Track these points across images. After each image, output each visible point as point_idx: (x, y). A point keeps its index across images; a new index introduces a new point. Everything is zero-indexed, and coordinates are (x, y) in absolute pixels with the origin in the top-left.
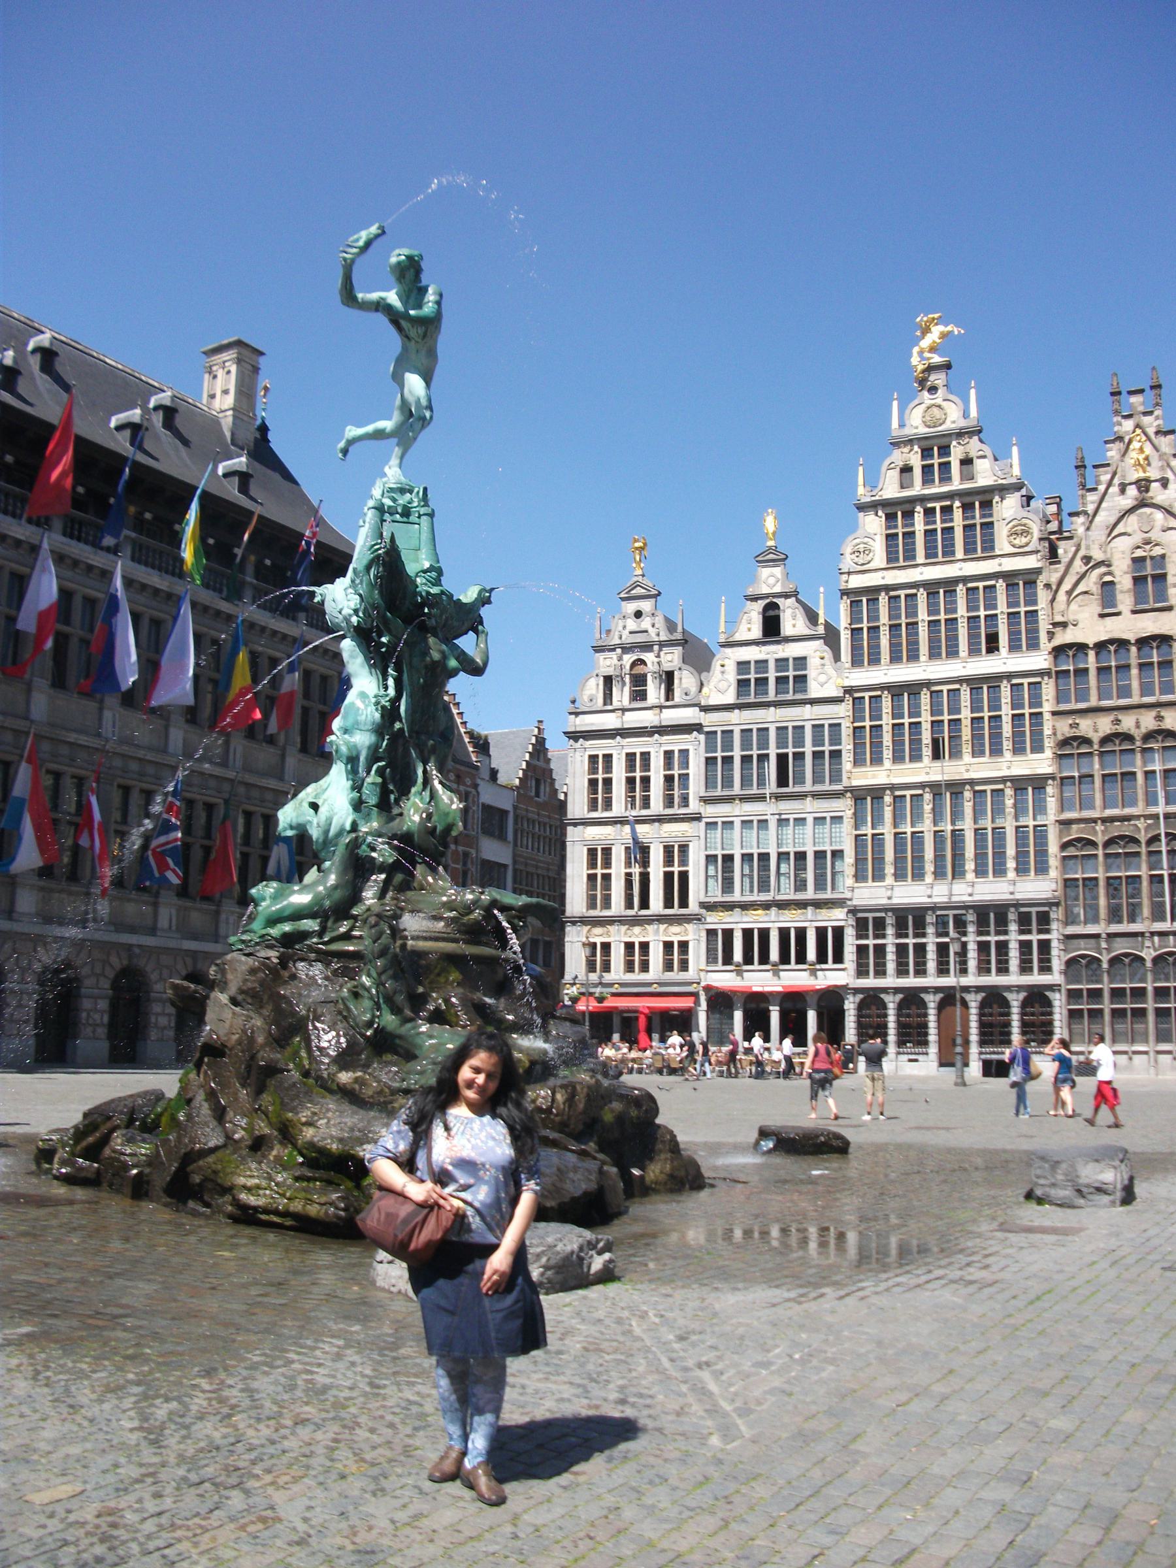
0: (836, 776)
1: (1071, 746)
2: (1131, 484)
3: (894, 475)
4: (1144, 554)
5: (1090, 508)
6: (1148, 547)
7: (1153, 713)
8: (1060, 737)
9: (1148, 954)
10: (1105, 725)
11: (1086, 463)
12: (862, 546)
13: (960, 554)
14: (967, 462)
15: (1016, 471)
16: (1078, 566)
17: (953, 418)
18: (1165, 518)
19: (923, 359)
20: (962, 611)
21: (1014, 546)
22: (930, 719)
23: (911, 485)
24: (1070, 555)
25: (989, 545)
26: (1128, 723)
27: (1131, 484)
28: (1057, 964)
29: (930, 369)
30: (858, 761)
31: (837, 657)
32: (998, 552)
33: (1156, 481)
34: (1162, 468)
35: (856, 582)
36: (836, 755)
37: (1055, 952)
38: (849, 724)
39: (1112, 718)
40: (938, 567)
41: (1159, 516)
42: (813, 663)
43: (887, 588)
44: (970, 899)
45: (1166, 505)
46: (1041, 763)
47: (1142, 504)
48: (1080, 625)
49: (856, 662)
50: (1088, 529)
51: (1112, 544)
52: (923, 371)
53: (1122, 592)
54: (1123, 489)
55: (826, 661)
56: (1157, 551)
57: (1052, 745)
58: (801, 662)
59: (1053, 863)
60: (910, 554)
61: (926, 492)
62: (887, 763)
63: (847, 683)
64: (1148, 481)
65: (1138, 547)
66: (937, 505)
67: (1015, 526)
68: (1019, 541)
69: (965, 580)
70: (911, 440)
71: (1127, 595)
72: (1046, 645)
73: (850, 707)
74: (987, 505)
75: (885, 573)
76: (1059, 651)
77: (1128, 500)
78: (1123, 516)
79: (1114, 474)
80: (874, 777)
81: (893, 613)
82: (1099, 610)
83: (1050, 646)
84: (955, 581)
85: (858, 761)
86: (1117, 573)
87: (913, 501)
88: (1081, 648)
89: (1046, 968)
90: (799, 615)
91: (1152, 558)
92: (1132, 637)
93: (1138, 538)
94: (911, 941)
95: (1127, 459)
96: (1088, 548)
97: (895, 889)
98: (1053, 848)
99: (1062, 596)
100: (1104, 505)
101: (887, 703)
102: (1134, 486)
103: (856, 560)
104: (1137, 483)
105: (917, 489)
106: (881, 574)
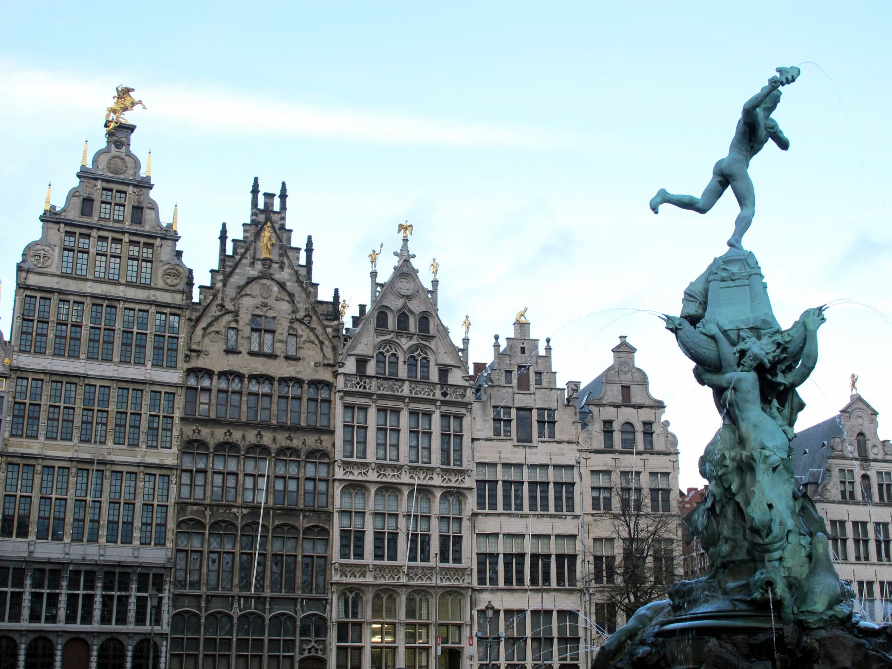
1: (192, 446)
2: (259, 260)
3: (78, 202)
4: (261, 313)
5: (228, 270)
6: (265, 309)
7: (256, 432)
8: (185, 438)
9: (236, 613)
10: (220, 434)
12: (42, 252)
14: (138, 210)
16: (214, 311)
18: (279, 292)
21: (167, 284)
22: (82, 406)
23: (90, 215)
24: (208, 301)
26: (237, 435)
27: (259, 260)
28: (166, 617)
33: (276, 263)
34: (281, 255)
35: (34, 280)
37: (165, 608)
38: (11, 399)
39: (225, 430)
40: (103, 285)
41: (275, 289)
43: (60, 292)
44: (101, 558)
45: (281, 281)
46: (169, 457)
47: (264, 275)
48: (210, 356)
50: (224, 285)
51: (240, 302)
52: (115, 128)
53: (243, 338)
54: (252, 264)
56: (271, 314)
57: (179, 443)
59: (170, 536)
62: (42, 438)
63: (15, 363)
64: (271, 260)
65: (258, 307)
66: (110, 235)
67: (168, 269)
68: (171, 281)
69: (126, 300)
71: (246, 340)
72: (183, 366)
73: (15, 384)
75: (59, 279)
76: (190, 372)
77: (253, 273)
78: (250, 282)
79: (247, 250)
80: (28, 447)
82: (225, 347)
83: (186, 366)
84: (117, 300)
86: (241, 323)
88: (209, 373)
89: (158, 621)
91: (266, 317)
92: (246, 372)
93: (259, 301)
94: (45, 591)
95: (258, 242)
96: (223, 299)
97: (38, 545)
98: (171, 525)
99: (199, 331)
100: (237, 270)
101: (114, 394)
102: (260, 262)
103: (35, 263)
104: (265, 259)
106: (56, 279)
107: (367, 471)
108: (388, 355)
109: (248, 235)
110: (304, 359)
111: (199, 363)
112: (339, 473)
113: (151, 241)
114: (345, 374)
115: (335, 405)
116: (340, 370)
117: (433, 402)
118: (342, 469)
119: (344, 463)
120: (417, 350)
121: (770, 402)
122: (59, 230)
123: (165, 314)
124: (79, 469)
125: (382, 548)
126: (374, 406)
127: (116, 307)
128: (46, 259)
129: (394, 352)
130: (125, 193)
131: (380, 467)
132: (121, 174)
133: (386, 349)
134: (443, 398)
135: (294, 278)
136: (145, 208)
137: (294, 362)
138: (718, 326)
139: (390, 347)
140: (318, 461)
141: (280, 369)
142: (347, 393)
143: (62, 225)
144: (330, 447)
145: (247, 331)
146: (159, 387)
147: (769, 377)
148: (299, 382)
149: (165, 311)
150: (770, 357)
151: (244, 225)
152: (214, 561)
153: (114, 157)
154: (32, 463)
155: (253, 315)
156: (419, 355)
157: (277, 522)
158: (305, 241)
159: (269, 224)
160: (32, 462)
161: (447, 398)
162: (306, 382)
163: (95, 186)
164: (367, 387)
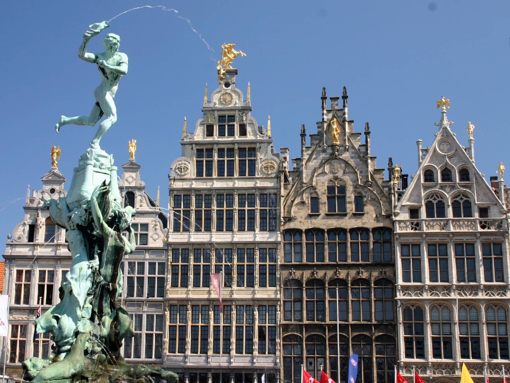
0: (162, 292)
11: (306, 133)
12: (183, 165)
13: (236, 175)
15: (269, 133)
17: (237, 102)
18: (346, 167)
19: (223, 67)
20: (236, 207)
25: (252, 172)
29: (229, 72)
30: (174, 285)
31: (165, 226)
32: (257, 176)
35: (178, 185)
36: (162, 281)
42: (151, 227)
47: (333, 157)
48: (299, 219)
49: (177, 229)
55: (158, 227)
58: (145, 226)
60: (209, 174)
61: (220, 139)
62: (190, 287)
63: (171, 240)
70: (214, 111)
74: (253, 151)
75: (194, 182)
81: (198, 205)
85: (174, 285)
87: (212, 143)
88: (298, 232)
90: (144, 201)
93: (331, 176)
102: (330, 148)
105: (216, 138)
107: (422, 292)
108: (435, 202)
109: (320, 130)
110: (368, 213)
111: (292, 225)
112: (400, 296)
113: (253, 146)
114: (400, 222)
115: (394, 244)
116: (397, 218)
117: (474, 234)
118: (401, 292)
119: (402, 287)
120: (459, 196)
121: (94, 247)
122: (192, 149)
123: (266, 194)
124: (215, 306)
125: (439, 349)
126: (424, 242)
127: (232, 195)
128: (186, 169)
129: (440, 199)
130: (234, 116)
131: (432, 288)
132: (229, 104)
133: (433, 198)
134: (482, 230)
135: (357, 156)
136: (248, 125)
137: (360, 216)
138: (66, 203)
139: (437, 196)
140: (383, 287)
141: (349, 223)
142: (401, 235)
143: (194, 146)
144: (392, 276)
145: (324, 199)
146: (265, 245)
147: (89, 231)
148: (366, 230)
149: (266, 193)
150: (83, 219)
151: (317, 123)
152: (311, 363)
153: (223, 94)
154: (184, 304)
155: (328, 187)
156: (461, 199)
157: (356, 334)
158: (364, 126)
159: (335, 120)
160: (185, 303)
161: (486, 230)
162: (371, 230)
163: (214, 115)
164: (418, 228)
